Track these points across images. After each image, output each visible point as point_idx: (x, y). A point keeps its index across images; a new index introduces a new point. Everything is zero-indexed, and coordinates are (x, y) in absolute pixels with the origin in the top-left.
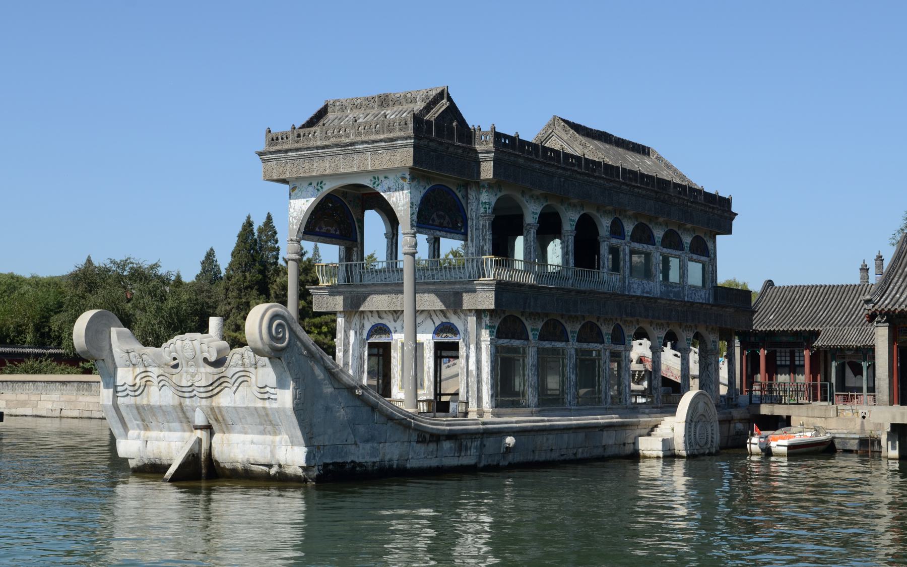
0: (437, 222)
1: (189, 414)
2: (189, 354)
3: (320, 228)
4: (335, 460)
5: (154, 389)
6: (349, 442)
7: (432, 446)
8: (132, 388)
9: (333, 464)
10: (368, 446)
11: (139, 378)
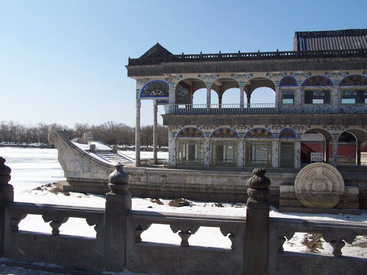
0: (155, 94)
4: (75, 177)
6: (80, 171)
10: (89, 174)
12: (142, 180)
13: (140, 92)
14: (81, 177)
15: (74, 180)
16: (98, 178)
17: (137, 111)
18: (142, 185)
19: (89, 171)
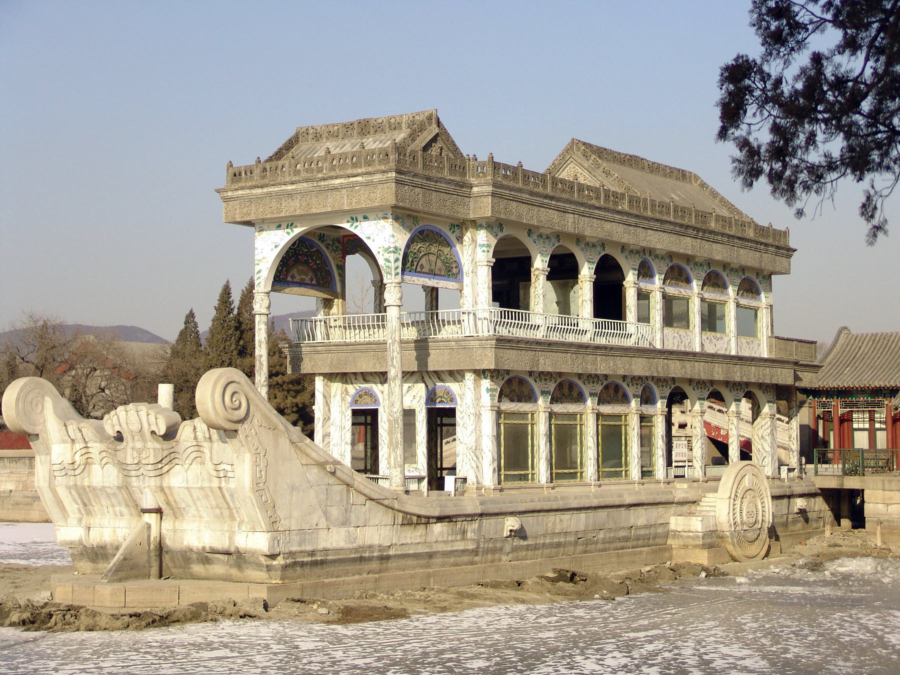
1: (137, 495)
2: (135, 427)
3: (293, 277)
4: (303, 548)
5: (96, 468)
7: (421, 530)
8: (71, 467)
10: (343, 531)
11: (79, 454)
12: (470, 535)
13: (401, 258)
14: (322, 545)
15: (298, 560)
16: (368, 542)
18: (457, 551)
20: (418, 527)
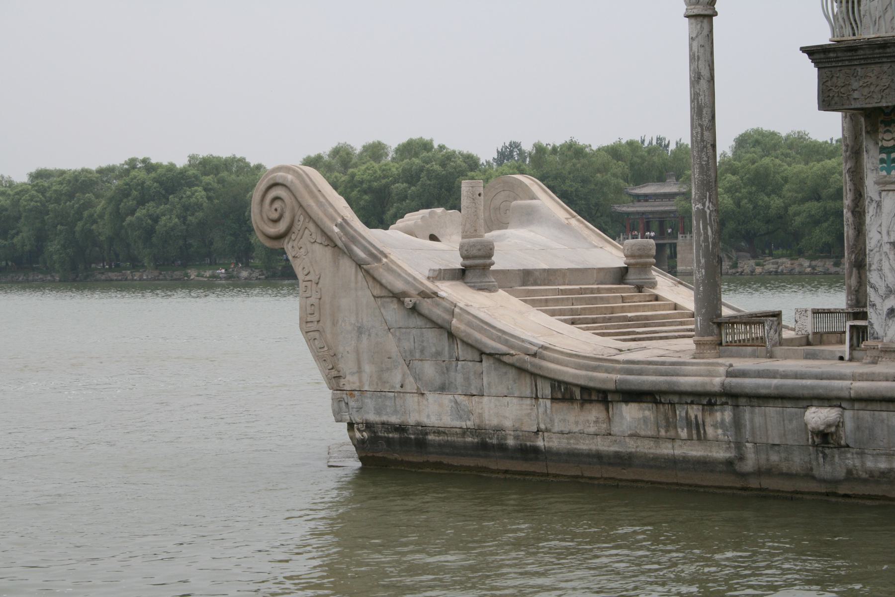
4: (384, 418)
6: (408, 388)
7: (595, 413)
9: (383, 424)
10: (446, 399)
12: (710, 431)
14: (411, 420)
17: (692, 39)
19: (443, 389)
20: (588, 406)
